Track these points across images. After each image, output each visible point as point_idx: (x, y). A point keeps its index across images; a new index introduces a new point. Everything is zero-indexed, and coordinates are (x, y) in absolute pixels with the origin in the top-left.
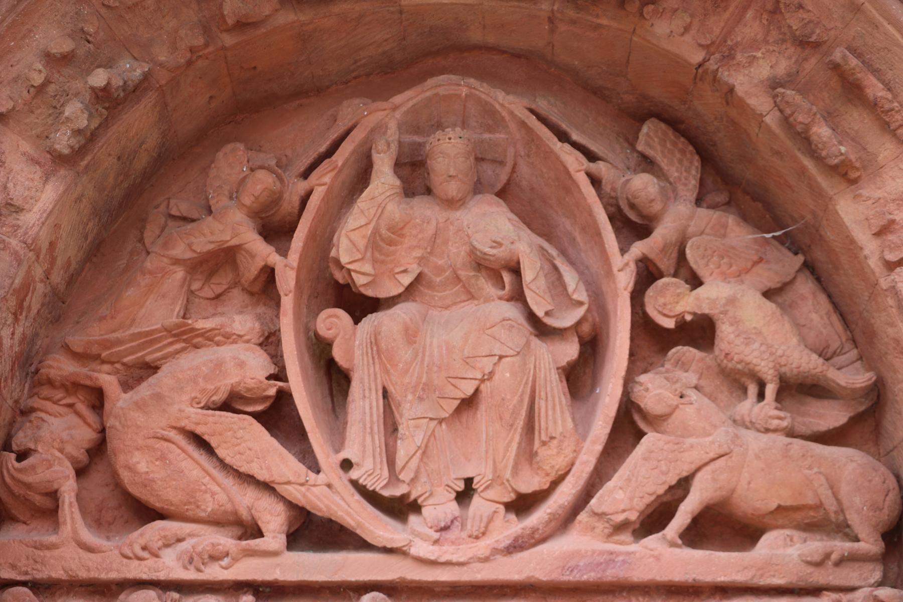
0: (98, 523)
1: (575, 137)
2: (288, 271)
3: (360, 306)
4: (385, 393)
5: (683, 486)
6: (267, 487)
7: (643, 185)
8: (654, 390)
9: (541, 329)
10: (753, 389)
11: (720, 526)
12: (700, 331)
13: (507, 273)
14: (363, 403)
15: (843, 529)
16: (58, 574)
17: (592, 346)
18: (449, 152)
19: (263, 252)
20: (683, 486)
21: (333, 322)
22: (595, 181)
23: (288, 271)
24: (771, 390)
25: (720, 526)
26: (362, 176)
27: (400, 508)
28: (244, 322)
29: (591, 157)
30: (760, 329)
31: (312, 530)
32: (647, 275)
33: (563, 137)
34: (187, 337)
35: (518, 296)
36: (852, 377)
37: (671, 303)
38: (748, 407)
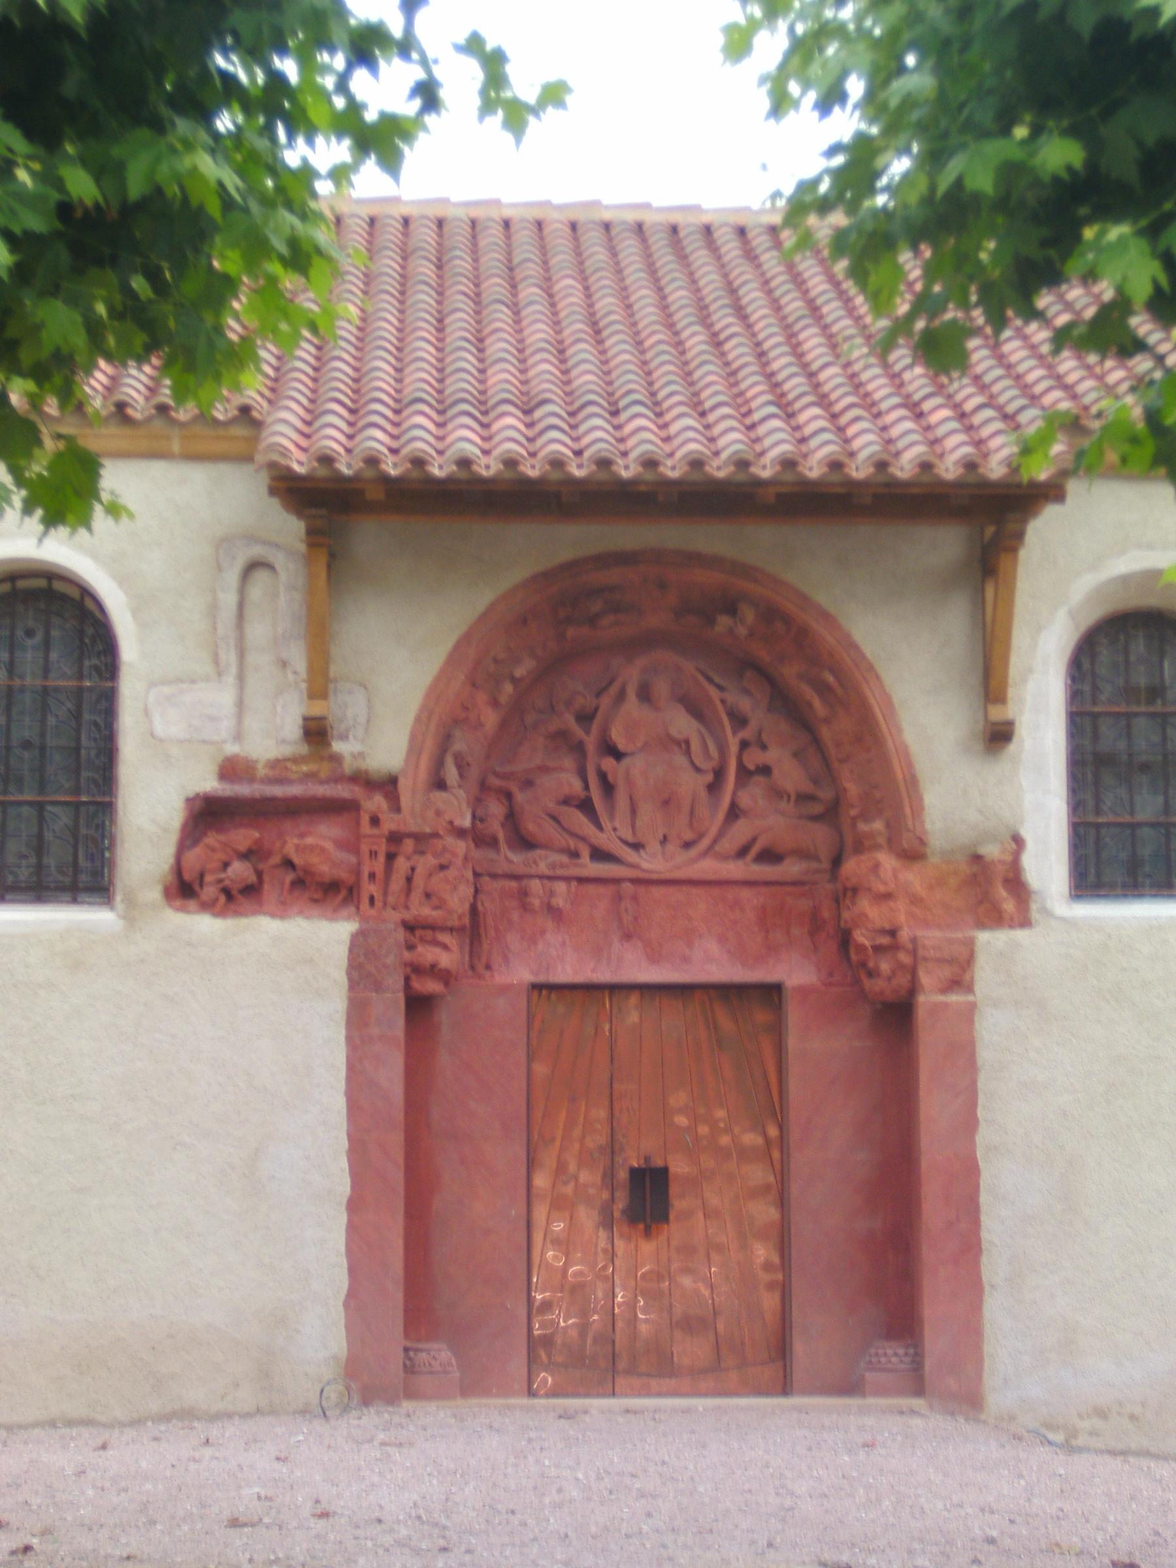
0: (511, 846)
1: (717, 679)
2: (591, 742)
3: (618, 755)
4: (631, 798)
5: (754, 840)
6: (583, 839)
7: (745, 704)
8: (745, 800)
9: (698, 770)
10: (785, 798)
11: (769, 856)
12: (765, 770)
13: (685, 745)
14: (622, 801)
15: (816, 858)
16: (500, 871)
17: (719, 774)
18: (662, 688)
19: (579, 732)
20: (754, 840)
21: (608, 763)
22: (723, 701)
23: (591, 742)
24: (793, 799)
25: (769, 856)
26: (621, 697)
27: (637, 846)
28: (569, 762)
29: (721, 688)
30: (790, 774)
31: (599, 855)
32: (744, 745)
33: (710, 680)
34: (544, 769)
35: (688, 752)
36: (826, 794)
37: (754, 758)
38: (783, 804)
